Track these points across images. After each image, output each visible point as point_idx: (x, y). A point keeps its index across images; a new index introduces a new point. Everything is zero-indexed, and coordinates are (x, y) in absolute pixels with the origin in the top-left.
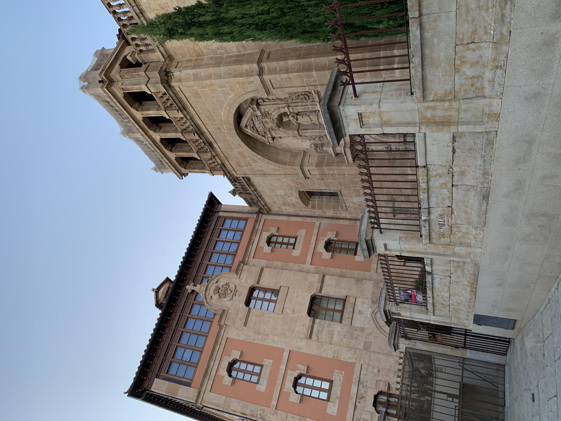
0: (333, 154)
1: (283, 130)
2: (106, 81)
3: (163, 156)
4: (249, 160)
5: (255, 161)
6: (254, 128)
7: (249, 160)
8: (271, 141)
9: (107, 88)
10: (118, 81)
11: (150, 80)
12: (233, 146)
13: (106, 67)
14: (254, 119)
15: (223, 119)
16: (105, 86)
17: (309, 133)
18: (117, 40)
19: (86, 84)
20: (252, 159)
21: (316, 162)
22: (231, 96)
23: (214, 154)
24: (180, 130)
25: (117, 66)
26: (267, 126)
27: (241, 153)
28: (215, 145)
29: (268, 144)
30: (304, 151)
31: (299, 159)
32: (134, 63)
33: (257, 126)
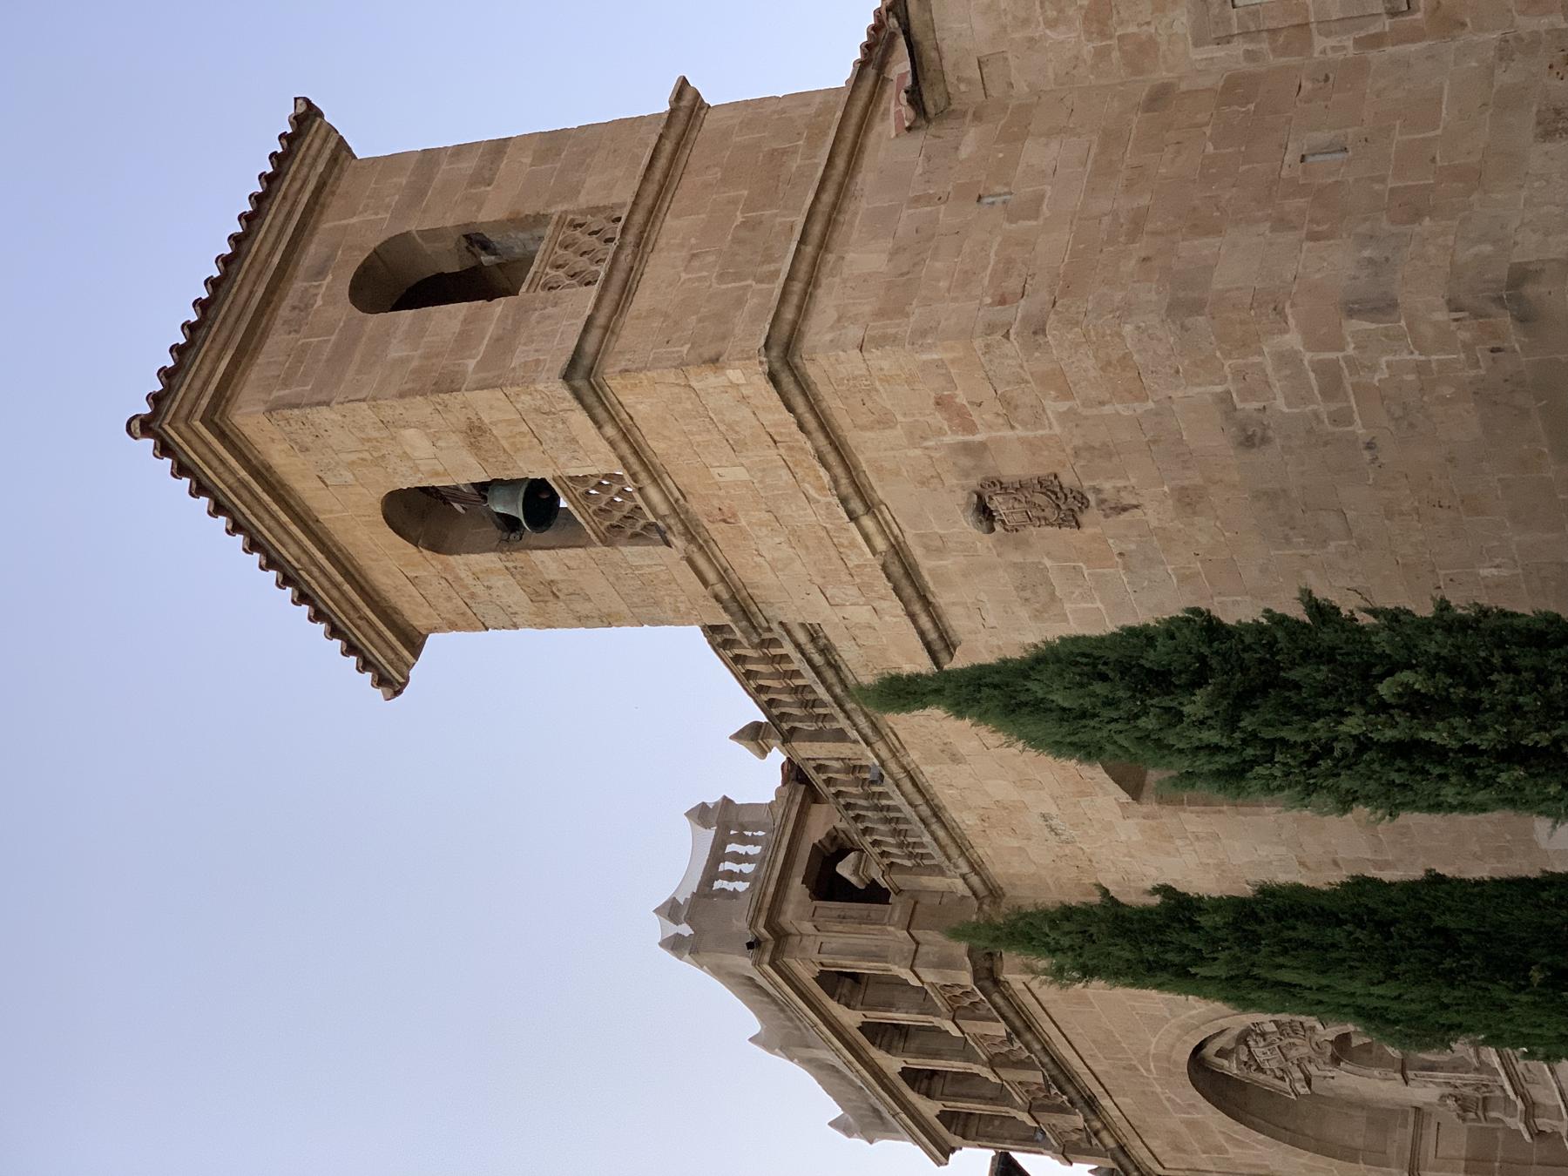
0: (1527, 1136)
1: (1349, 1067)
2: (767, 940)
3: (899, 1110)
4: (1221, 1139)
5: (1239, 1144)
6: (1252, 1063)
7: (1221, 1139)
8: (1304, 1091)
9: (772, 964)
10: (801, 934)
11: (922, 949)
12: (1168, 1105)
13: (765, 894)
14: (1251, 1043)
15: (1152, 1051)
16: (767, 958)
17: (1441, 1076)
18: (780, 784)
19: (685, 930)
20: (1229, 1139)
21: (1463, 1153)
22: (1194, 1012)
23: (1098, 1125)
24: (984, 1057)
25: (797, 888)
26: (1293, 1053)
27: (1191, 1124)
28: (1105, 1102)
29: (1293, 1097)
30: (1417, 1109)
31: (1403, 1136)
32: (862, 887)
33: (1260, 1058)
